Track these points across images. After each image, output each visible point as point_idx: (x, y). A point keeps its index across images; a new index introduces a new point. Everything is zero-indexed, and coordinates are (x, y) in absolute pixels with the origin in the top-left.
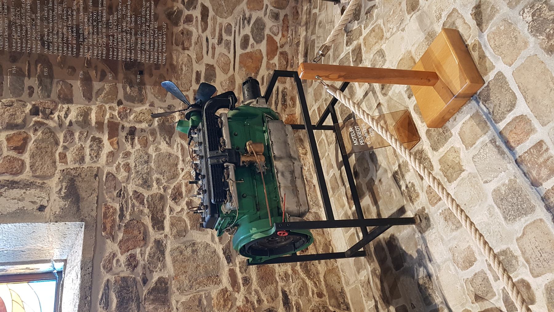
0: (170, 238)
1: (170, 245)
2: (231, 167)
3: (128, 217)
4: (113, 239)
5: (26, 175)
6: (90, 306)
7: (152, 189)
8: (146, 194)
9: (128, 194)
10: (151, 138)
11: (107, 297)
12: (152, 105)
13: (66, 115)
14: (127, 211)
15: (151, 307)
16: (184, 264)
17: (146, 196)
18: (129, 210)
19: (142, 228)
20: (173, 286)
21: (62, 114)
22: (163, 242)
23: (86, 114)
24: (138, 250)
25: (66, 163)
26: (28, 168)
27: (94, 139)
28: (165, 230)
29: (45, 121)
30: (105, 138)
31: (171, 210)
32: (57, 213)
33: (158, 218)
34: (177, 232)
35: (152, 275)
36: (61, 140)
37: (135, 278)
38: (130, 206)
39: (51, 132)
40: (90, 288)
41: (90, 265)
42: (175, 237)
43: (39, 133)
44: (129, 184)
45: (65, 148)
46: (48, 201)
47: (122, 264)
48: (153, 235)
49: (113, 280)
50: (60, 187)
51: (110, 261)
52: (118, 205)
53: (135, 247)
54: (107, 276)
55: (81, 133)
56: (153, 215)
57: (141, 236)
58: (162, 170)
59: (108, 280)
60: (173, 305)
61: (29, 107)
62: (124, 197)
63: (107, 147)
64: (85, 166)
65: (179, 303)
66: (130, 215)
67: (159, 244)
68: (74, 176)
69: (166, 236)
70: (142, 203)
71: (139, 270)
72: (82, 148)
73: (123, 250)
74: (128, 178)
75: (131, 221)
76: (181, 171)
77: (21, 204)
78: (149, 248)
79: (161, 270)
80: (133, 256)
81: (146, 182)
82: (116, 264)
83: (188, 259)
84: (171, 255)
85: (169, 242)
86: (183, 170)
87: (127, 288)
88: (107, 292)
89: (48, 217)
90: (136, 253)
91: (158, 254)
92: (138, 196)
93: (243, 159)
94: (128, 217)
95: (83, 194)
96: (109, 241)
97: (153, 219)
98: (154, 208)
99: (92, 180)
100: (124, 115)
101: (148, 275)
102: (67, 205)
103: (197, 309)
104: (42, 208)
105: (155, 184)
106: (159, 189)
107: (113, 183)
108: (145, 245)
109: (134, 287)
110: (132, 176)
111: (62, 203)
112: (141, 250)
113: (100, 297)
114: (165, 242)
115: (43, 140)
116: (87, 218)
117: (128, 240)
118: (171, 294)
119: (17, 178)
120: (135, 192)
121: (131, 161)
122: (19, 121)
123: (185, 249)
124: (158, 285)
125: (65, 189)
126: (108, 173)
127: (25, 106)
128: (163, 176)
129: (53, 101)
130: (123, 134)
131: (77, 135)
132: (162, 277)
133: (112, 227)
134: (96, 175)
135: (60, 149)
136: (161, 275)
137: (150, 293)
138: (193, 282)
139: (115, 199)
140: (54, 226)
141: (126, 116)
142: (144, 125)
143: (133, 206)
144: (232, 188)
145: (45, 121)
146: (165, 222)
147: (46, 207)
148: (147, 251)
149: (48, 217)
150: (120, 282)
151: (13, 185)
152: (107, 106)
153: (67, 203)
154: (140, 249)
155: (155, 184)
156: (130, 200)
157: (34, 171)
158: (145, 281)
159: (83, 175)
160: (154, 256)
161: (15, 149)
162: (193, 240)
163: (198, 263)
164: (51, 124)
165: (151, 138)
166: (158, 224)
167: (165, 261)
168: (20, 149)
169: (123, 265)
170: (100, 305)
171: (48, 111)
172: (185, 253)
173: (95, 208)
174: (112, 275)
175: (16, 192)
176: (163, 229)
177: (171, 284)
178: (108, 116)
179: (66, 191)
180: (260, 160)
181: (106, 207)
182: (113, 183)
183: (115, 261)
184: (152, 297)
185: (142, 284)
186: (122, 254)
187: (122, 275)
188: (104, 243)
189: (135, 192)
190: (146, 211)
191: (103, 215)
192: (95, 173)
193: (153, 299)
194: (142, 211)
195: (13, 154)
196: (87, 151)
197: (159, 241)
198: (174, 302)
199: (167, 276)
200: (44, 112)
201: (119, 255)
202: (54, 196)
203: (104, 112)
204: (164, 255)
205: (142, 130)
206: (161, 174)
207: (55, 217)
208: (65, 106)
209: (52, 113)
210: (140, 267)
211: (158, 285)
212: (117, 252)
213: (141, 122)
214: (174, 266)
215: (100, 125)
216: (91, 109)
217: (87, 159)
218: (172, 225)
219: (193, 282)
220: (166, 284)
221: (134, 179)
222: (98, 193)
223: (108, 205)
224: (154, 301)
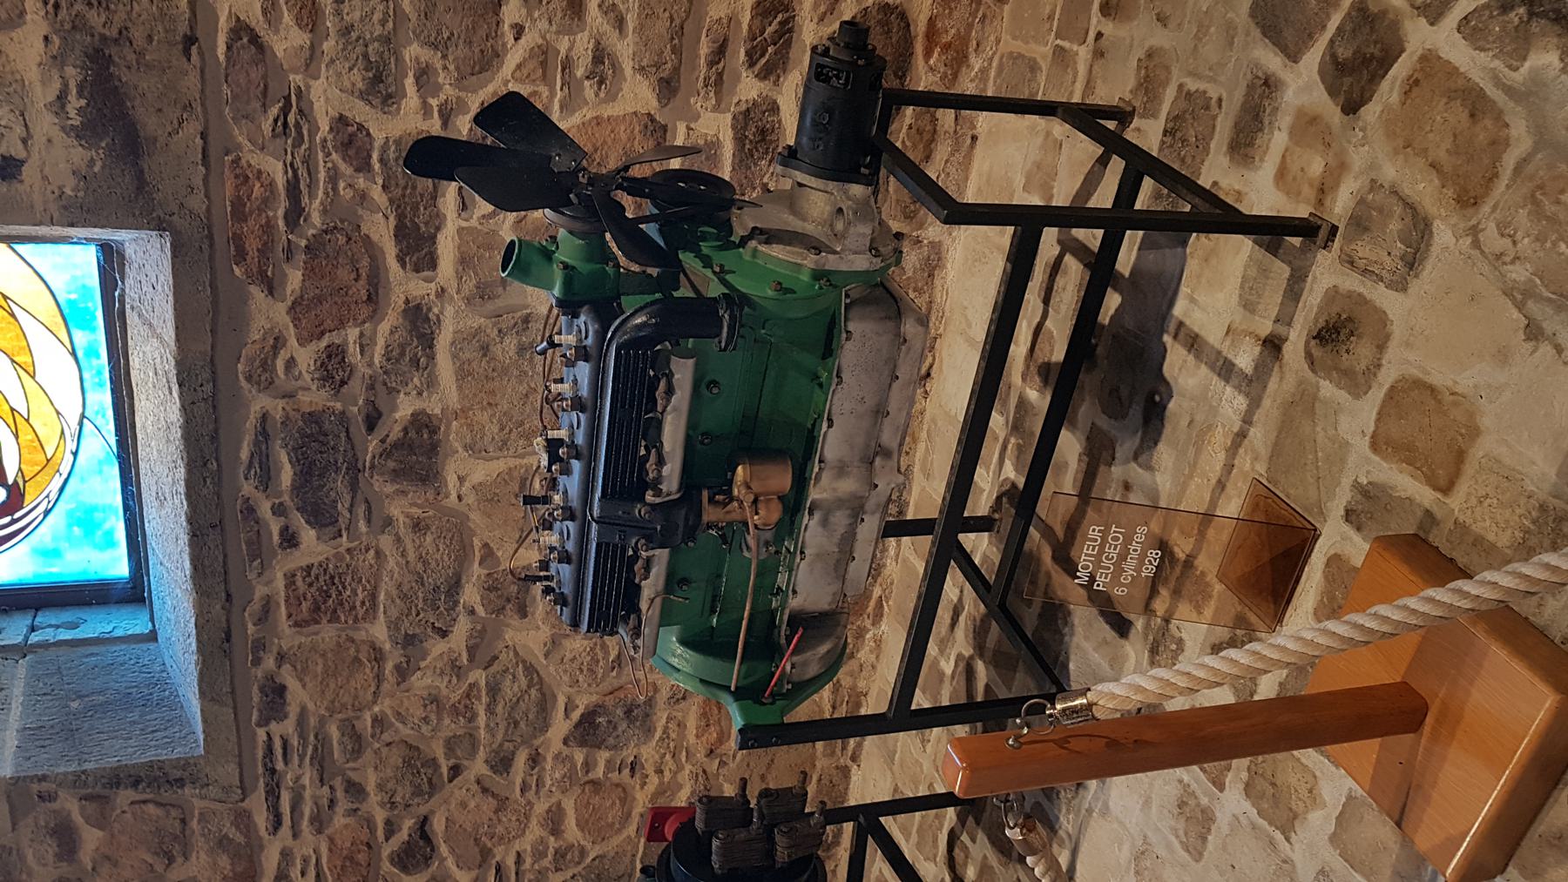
0: (452, 298)
1: (451, 324)
3: (316, 219)
4: (271, 287)
6: (218, 483)
7: (399, 109)
9: (314, 129)
11: (264, 460)
14: (312, 196)
15: (390, 488)
16: (489, 386)
17: (379, 137)
18: (321, 193)
19: (365, 263)
20: (454, 434)
22: (430, 309)
24: (352, 333)
28: (439, 269)
32: (68, 191)
33: (419, 228)
34: (478, 288)
35: (395, 399)
37: (343, 413)
38: (322, 175)
40: (214, 438)
41: (206, 375)
42: (469, 301)
44: (317, 78)
46: (24, 141)
47: (304, 372)
48: (403, 285)
49: (278, 416)
50: (56, 85)
51: (267, 365)
52: (280, 165)
53: (341, 324)
56: (400, 217)
57: (361, 290)
58: (439, 32)
59: (264, 417)
60: (451, 486)
62: (299, 139)
65: (467, 484)
66: (324, 212)
68: (104, 38)
69: (441, 292)
70: (364, 166)
71: (356, 387)
73: (305, 334)
74: (314, 51)
75: (326, 232)
76: (509, 38)
78: (384, 328)
79: (420, 394)
80: (335, 354)
81: (378, 79)
82: (286, 375)
83: (505, 371)
84: (455, 356)
85: (449, 311)
86: (519, 31)
87: (321, 438)
88: (264, 447)
89: (39, 207)
90: (346, 342)
91: (415, 347)
94: (316, 219)
95: (150, 123)
96: (257, 293)
97: (400, 233)
98: (405, 188)
99: (175, 62)
101: (382, 404)
102: (99, 164)
103: (514, 501)
105: (409, 82)
106: (426, 110)
107: (255, 74)
108: (375, 315)
109: (343, 435)
110: (326, 46)
111: (79, 155)
112: (362, 335)
113: (244, 454)
114: (436, 310)
116: (175, 218)
117: (319, 300)
118: (446, 456)
120: (341, 121)
123: (498, 340)
124: (412, 434)
125: (80, 95)
128: (444, 57)
132: (423, 412)
133: (265, 251)
134: (190, 40)
136: (419, 405)
137: (386, 454)
138: (511, 430)
139: (267, 143)
143: (333, 177)
146: (440, 237)
147: (22, 162)
148: (379, 335)
149: (39, 207)
150: (300, 423)
153: (99, 156)
154: (357, 331)
155: (409, 82)
156: (321, 155)
158: (372, 420)
159: (138, 34)
160: (402, 354)
162: (527, 307)
163: (533, 385)
167: (435, 365)
169: (308, 377)
170: (246, 479)
172: (497, 350)
173: (198, 181)
174: (276, 398)
176: (432, 263)
177: (447, 434)
179: (83, 102)
181: (237, 177)
182: (255, 74)
183: (280, 364)
184: (391, 464)
185: (364, 431)
186: (302, 342)
188: (244, 299)
189: (341, 121)
190: (377, 194)
191: (229, 209)
192: (183, 28)
193: (394, 470)
194: (363, 197)
197: (418, 307)
198: (452, 480)
199: (437, 411)
201: (293, 342)
202: (45, 124)
204: (431, 347)
206: (436, 48)
207: (65, 208)
210: (359, 382)
211: (412, 434)
212: (287, 329)
214: (460, 388)
218: (464, 261)
219: (511, 430)
220: (434, 431)
221: (332, 61)
222: (207, 121)
223: (243, 162)
224: (396, 475)
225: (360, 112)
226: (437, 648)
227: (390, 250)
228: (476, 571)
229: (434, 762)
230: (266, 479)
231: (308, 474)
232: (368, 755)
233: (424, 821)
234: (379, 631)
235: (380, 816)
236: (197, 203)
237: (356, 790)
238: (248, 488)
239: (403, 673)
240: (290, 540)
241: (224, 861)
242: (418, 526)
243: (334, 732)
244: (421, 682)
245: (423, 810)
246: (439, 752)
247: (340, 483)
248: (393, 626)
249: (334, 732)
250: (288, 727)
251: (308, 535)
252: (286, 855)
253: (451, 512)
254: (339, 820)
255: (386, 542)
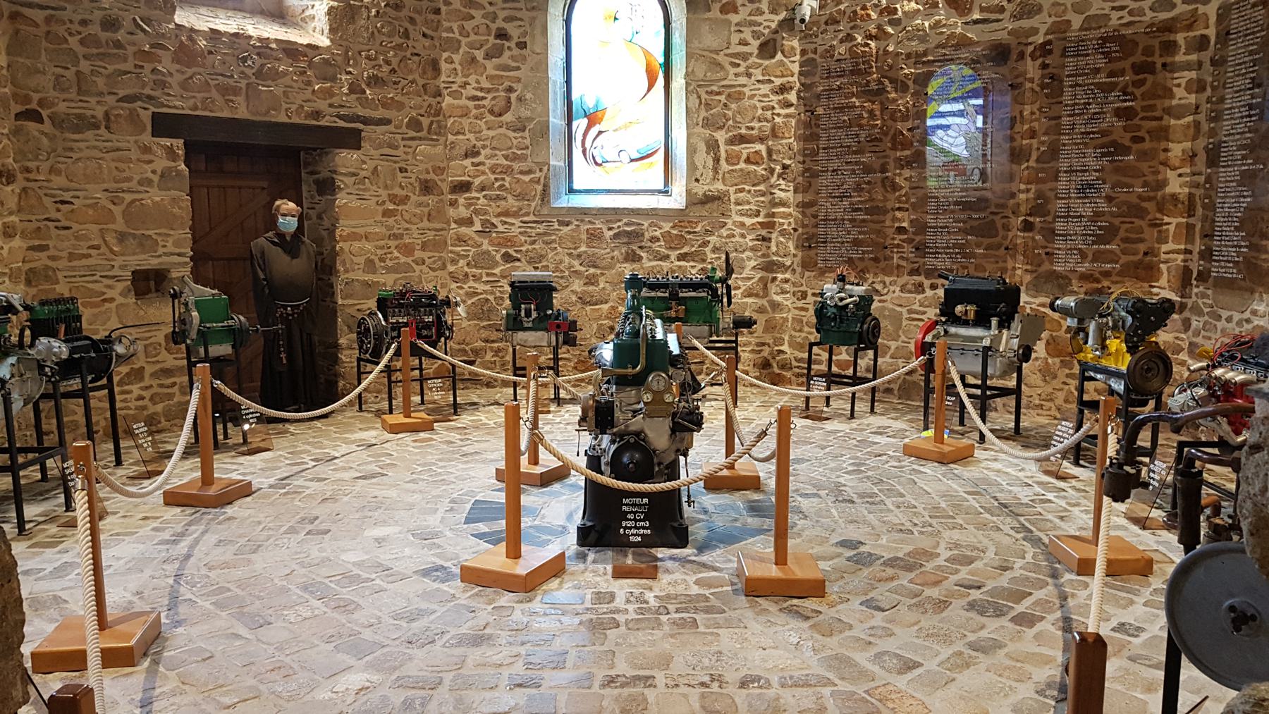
2: (667, 295)
4: (673, 227)
5: (724, 166)
8: (708, 250)
10: (759, 254)
12: (795, 256)
13: (782, 190)
21: (783, 187)
23: (783, 204)
25: (736, 193)
26: (731, 168)
27: (759, 211)
29: (775, 175)
30: (760, 219)
31: (693, 267)
36: (758, 188)
39: (765, 180)
43: (764, 172)
45: (749, 191)
51: (655, 226)
54: (646, 224)
55: (763, 202)
61: (788, 162)
63: (749, 221)
64: (732, 206)
67: (667, 257)
70: (700, 246)
71: (649, 244)
72: (749, 203)
77: (700, 167)
80: (658, 240)
91: (659, 257)
92: (705, 244)
93: (674, 303)
95: (707, 206)
100: (783, 233)
104: (697, 180)
108: (667, 248)
111: (700, 193)
115: (756, 176)
119: (723, 162)
121: (737, 239)
122: (774, 157)
126: (726, 224)
127: (790, 159)
129: (795, 179)
130: (764, 233)
131: (762, 199)
135: (747, 188)
137: (633, 250)
140: (684, 189)
141: (783, 235)
142: (774, 249)
144: (653, 294)
145: (775, 175)
151: (717, 160)
152: (792, 220)
157: (728, 172)
161: (748, 158)
164: (773, 180)
165: (759, 254)
166: (682, 257)
168: (748, 161)
171: (785, 176)
175: (710, 163)
178: (781, 220)
180: (673, 314)
187: (646, 233)
190: (693, 249)
195: (744, 156)
196: (747, 207)
200: (783, 173)
202: (706, 188)
203: (786, 218)
205: (769, 248)
208: (792, 188)
209: (784, 179)
213: (777, 246)
215: (773, 215)
216: (789, 207)
217: (740, 208)
218: (680, 267)
224: (627, 253)
225: (711, 246)
226: (576, 263)
227: (682, 252)
228: (599, 272)
229: (540, 262)
230: (627, 224)
231: (628, 234)
232: (544, 246)
233: (519, 260)
234: (583, 248)
235: (523, 249)
236: (691, 214)
237: (533, 242)
238: (625, 220)
239: (570, 255)
240: (610, 229)
241: (515, 209)
242: (613, 257)
243: (553, 237)
244: (567, 259)
245: (523, 260)
246: (544, 263)
247: (625, 240)
248: (585, 252)
249: (553, 237)
250: (556, 226)
251: (611, 233)
252: (513, 224)
253: (615, 265)
254: (523, 239)
255: (608, 250)
